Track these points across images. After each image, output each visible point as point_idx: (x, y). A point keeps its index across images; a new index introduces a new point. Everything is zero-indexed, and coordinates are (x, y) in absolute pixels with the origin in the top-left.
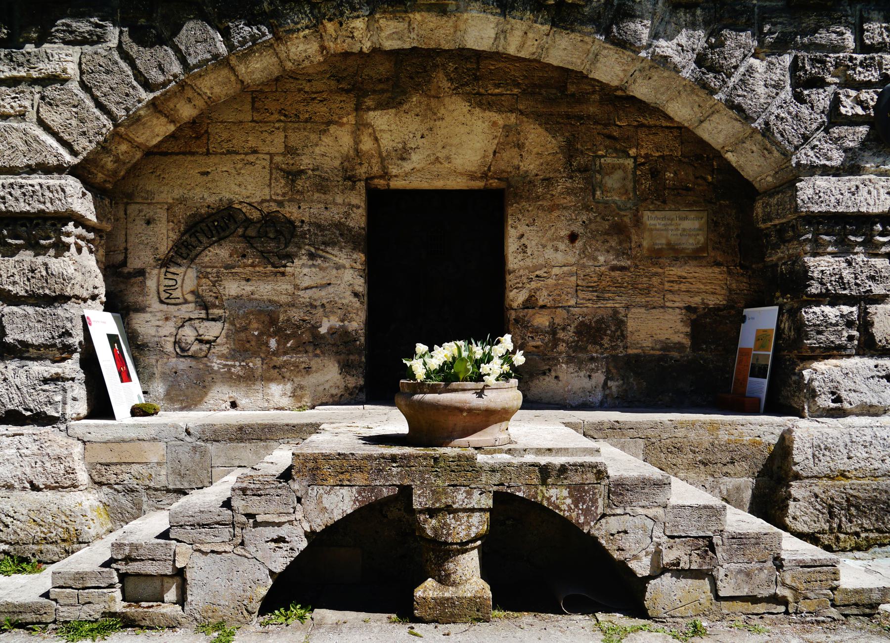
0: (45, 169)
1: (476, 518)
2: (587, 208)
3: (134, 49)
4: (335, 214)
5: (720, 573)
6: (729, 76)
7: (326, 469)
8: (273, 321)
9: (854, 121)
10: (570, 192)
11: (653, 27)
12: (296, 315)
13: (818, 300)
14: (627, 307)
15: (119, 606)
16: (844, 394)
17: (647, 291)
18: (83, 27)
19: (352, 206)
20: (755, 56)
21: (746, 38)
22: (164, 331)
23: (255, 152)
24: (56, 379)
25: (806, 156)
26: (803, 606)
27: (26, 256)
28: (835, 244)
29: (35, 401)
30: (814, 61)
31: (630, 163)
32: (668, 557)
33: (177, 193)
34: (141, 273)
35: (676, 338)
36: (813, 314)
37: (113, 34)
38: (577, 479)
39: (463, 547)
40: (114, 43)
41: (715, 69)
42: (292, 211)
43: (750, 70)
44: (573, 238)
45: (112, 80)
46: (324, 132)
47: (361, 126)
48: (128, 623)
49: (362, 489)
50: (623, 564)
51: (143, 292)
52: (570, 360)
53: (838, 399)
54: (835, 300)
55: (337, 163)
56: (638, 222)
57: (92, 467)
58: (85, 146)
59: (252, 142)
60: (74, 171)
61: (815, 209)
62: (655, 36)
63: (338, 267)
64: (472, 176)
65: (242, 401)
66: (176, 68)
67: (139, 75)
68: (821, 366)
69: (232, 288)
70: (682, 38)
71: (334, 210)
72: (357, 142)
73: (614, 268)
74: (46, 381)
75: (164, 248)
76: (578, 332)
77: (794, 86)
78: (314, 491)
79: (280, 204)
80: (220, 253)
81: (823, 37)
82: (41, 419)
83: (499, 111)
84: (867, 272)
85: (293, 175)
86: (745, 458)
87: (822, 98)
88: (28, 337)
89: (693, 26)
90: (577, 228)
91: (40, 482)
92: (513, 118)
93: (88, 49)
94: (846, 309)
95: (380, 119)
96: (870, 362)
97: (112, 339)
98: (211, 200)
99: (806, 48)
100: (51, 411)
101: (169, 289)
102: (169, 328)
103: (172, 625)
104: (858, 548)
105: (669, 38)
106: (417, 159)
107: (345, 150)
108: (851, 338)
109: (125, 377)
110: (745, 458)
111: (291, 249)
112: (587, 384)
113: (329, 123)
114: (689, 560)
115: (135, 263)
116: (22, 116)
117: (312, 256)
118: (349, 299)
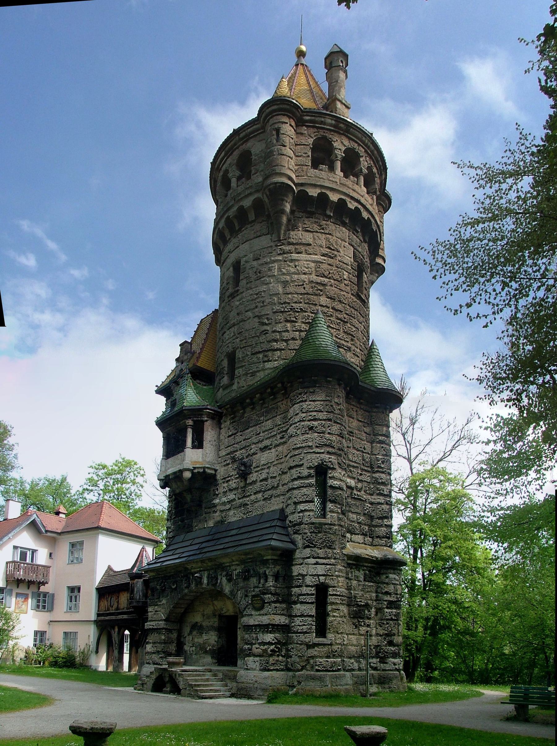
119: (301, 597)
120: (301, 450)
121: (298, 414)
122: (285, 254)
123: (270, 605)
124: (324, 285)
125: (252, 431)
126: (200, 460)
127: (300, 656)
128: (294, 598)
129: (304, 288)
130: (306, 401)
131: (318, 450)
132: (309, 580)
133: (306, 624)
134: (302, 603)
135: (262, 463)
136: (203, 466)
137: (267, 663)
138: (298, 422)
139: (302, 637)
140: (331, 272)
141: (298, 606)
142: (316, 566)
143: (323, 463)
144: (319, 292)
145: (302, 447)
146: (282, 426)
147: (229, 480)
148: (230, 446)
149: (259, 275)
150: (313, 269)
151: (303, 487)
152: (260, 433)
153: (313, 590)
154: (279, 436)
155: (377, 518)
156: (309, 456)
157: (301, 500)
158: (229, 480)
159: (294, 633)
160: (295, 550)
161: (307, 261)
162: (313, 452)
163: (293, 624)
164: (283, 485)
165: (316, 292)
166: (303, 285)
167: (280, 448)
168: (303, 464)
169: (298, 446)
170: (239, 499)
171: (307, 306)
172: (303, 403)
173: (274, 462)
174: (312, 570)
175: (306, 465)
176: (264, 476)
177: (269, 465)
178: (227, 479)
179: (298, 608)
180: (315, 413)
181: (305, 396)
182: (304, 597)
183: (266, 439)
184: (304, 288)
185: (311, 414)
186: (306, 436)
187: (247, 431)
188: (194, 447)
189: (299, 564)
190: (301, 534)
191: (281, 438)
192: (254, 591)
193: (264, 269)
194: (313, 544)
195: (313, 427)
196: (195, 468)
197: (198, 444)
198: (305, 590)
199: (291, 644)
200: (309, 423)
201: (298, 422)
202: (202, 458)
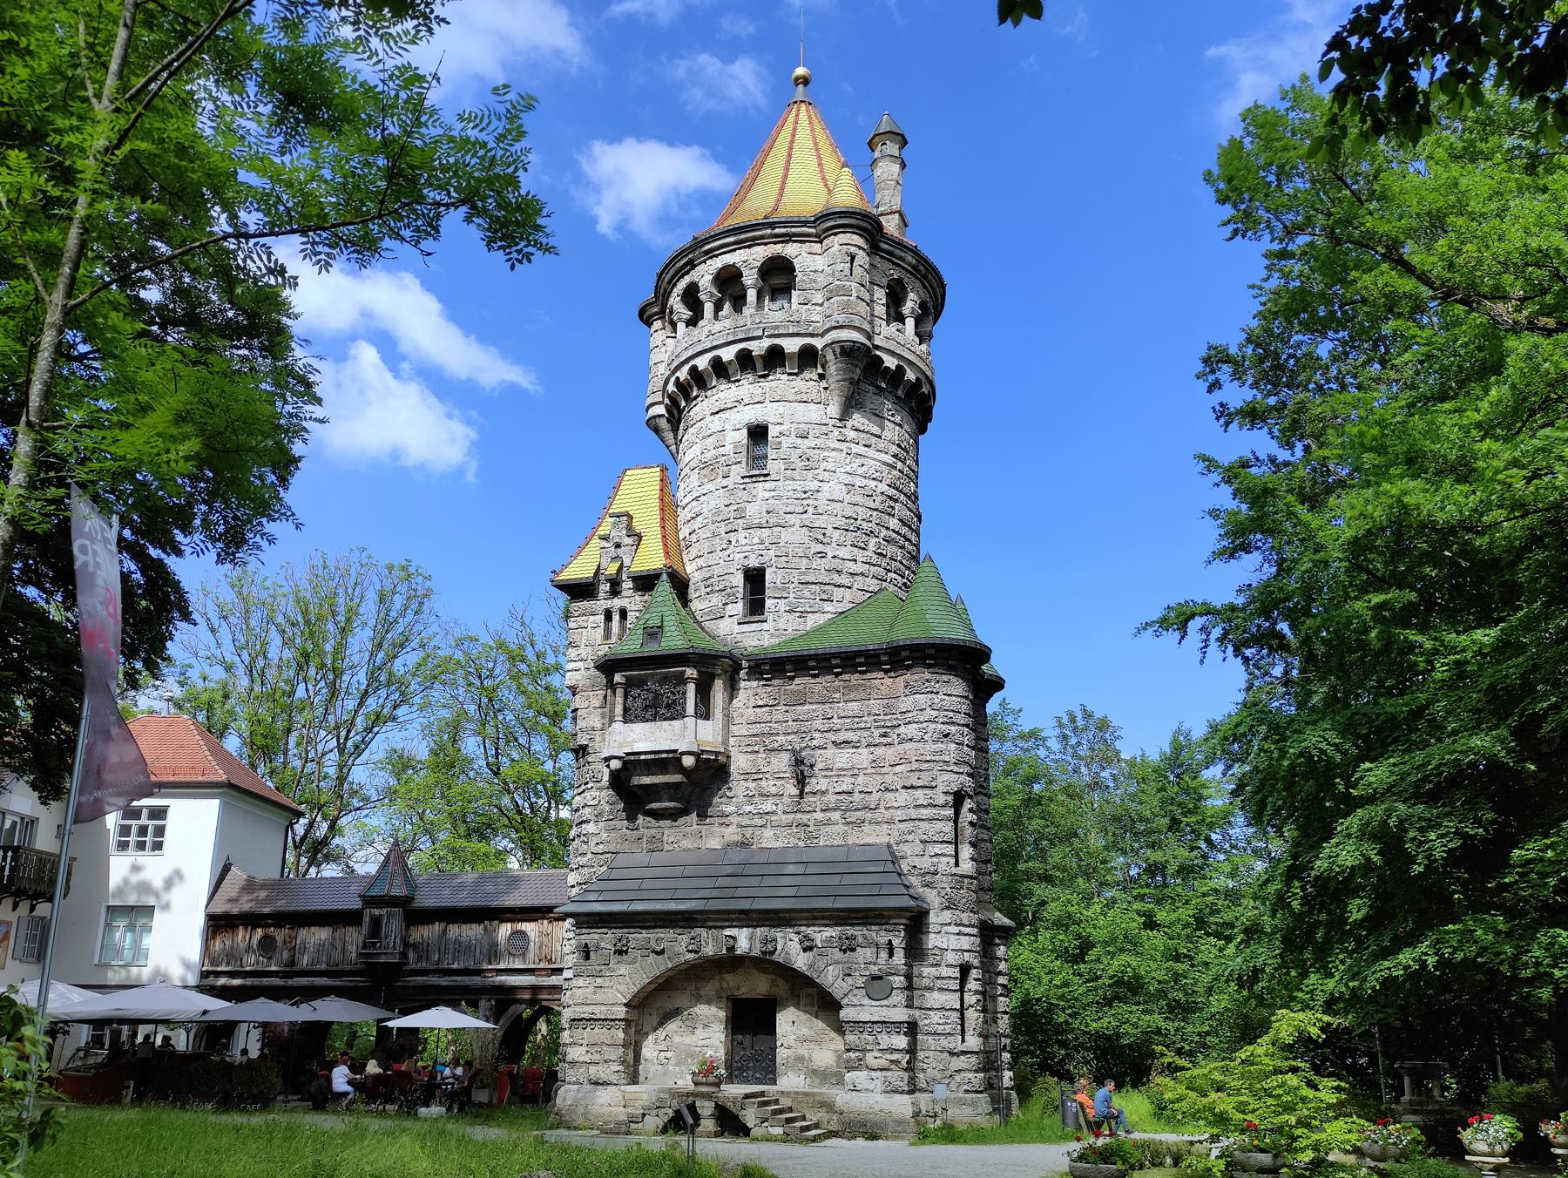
58: (629, 997)
87: (850, 980)
95: (728, 977)
106: (744, 990)
124: (896, 501)
125: (814, 711)
128: (926, 982)
131: (956, 769)
132: (951, 957)
134: (941, 989)
135: (841, 765)
139: (944, 1042)
141: (936, 994)
146: (882, 717)
153: (956, 973)
154: (876, 733)
156: (946, 776)
160: (927, 912)
163: (926, 1022)
164: (887, 808)
167: (880, 751)
170: (785, 812)
171: (877, 528)
174: (954, 942)
175: (941, 788)
176: (844, 788)
177: (856, 771)
179: (935, 999)
180: (951, 714)
186: (940, 745)
187: (799, 708)
188: (698, 715)
191: (881, 736)
197: (704, 712)
198: (945, 972)
200: (944, 727)
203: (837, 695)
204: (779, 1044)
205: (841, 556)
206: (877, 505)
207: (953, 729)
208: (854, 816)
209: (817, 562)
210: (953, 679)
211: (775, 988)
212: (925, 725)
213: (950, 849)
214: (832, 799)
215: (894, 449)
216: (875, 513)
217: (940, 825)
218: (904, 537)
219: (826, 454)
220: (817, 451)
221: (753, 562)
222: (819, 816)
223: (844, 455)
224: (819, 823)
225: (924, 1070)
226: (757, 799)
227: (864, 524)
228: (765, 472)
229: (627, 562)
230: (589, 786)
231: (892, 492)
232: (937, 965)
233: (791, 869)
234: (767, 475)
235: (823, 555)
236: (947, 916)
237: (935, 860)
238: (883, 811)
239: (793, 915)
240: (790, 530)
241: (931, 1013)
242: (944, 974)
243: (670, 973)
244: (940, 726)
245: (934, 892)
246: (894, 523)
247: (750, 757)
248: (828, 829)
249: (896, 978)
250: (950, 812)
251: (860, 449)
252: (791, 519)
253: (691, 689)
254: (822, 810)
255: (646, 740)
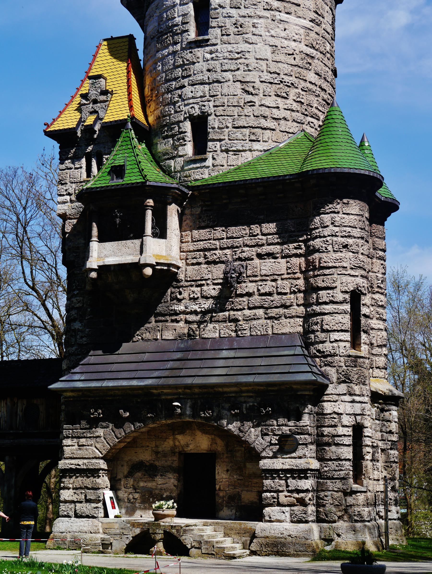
0: (96, 458)
1: (160, 535)
2: (231, 462)
3: (115, 429)
4: (169, 463)
5: (202, 548)
6: (245, 433)
7: (136, 525)
8: (151, 493)
9: (275, 444)
10: (227, 457)
11: (227, 422)
12: (157, 492)
13: (267, 491)
14: (242, 491)
15: (101, 549)
16: (271, 516)
17: (247, 486)
18: (104, 424)
19: (174, 461)
20: (253, 428)
21: (250, 424)
22: (125, 496)
23: (148, 446)
24: (97, 508)
25: (264, 454)
26: (218, 556)
27: (92, 478)
28: (271, 477)
29: (92, 513)
30: (266, 429)
31: (243, 449)
32: (193, 544)
33: (129, 458)
34: (120, 480)
35: (255, 500)
36: (265, 495)
37: (111, 425)
38: (177, 528)
39: (158, 541)
40: (111, 428)
41: (242, 432)
42: (157, 463)
43: (251, 432)
44: (228, 471)
45: (110, 437)
46: (165, 441)
47: (174, 439)
48: (102, 552)
49: (142, 528)
50: (185, 545)
51: (120, 485)
52: (226, 506)
53: (270, 518)
54: (270, 492)
55: (169, 449)
56: (245, 466)
57: (103, 529)
58: (104, 452)
59: (147, 444)
60: (102, 458)
61: (264, 468)
62: (228, 424)
63: (169, 478)
64: (207, 450)
65: (143, 516)
66: (123, 434)
67: (116, 436)
68: (267, 509)
69: (142, 484)
70: (234, 424)
71: (168, 462)
72: (174, 443)
73: (238, 480)
74: (94, 508)
75: (126, 473)
76: (228, 498)
77: (262, 435)
78: (134, 529)
79: (154, 461)
80: (139, 474)
81: (268, 422)
82: (93, 517)
83: (209, 434)
84: (278, 484)
85: (157, 453)
86: (248, 532)
87: (268, 438)
88: (91, 498)
89: (237, 421)
90: (229, 468)
91: (92, 531)
92: (213, 436)
93: (105, 429)
94: (272, 494)
95: (179, 437)
96: (279, 508)
97: (111, 498)
98: (137, 460)
99: (265, 425)
100: (95, 515)
101: (127, 484)
102: (126, 495)
103: (110, 553)
104: (266, 555)
105: (231, 424)
106: (191, 447)
107: (171, 445)
108: (274, 502)
109: (114, 507)
110: (248, 532)
111: (156, 474)
112: (230, 513)
113: (166, 438)
114: (197, 545)
115: (119, 477)
116: (91, 445)
117: (161, 475)
118: (173, 487)
119: (336, 438)
120: (334, 270)
121: (327, 226)
122: (272, 10)
123: (307, 447)
124: (313, 57)
126: (164, 253)
127: (338, 505)
129: (295, 58)
130: (338, 213)
131: (352, 273)
133: (343, 469)
135: (263, 272)
136: (169, 262)
137: (305, 514)
138: (329, 236)
140: (318, 42)
141: (333, 448)
142: (351, 404)
143: (357, 288)
144: (308, 65)
145: (335, 267)
147: (203, 285)
148: (202, 240)
149: (240, 29)
150: (303, 37)
151: (337, 313)
152: (258, 234)
153: (349, 431)
155: (378, 346)
156: (345, 279)
157: (335, 328)
158: (203, 285)
159: (329, 478)
160: (327, 386)
161: (297, 25)
162: (349, 274)
165: (306, 65)
166: (293, 54)
168: (336, 287)
169: (330, 265)
171: (296, 80)
172: (336, 215)
173: (283, 274)
176: (267, 290)
177: (276, 277)
178: (200, 282)
181: (338, 206)
182: (341, 438)
183: (269, 244)
184: (295, 58)
185: (345, 229)
186: (339, 254)
188: (155, 235)
189: (334, 401)
190: (335, 366)
191: (296, 248)
192: (278, 430)
193: (247, 22)
194: (349, 379)
195: (347, 245)
196: (158, 264)
199: (324, 491)
200: (343, 240)
201: (329, 236)
202: (166, 251)
203: (262, 217)
204: (217, 487)
205: (267, 104)
206: (298, 61)
207: (350, 241)
208: (273, 312)
209: (248, 110)
210: (351, 201)
211: (214, 445)
212: (328, 238)
213: (347, 336)
214: (256, 299)
215: (313, 16)
216: (296, 68)
217: (339, 317)
218: (320, 87)
219: (255, 21)
220: (247, 19)
221: (196, 112)
222: (247, 312)
223: (269, 21)
224: (247, 320)
225: (324, 506)
226: (200, 300)
227: (286, 79)
228: (206, 37)
229: (101, 114)
230: (76, 292)
231: (310, 51)
232: (335, 426)
233: (225, 354)
234: (208, 40)
235: (252, 104)
236: (343, 388)
237: (335, 344)
238: (296, 307)
239: (226, 389)
240: (226, 84)
241: (330, 462)
242: (340, 433)
243: (135, 434)
244: (340, 239)
245: (334, 370)
246: (311, 76)
247: (196, 267)
248: (255, 322)
249: (302, 436)
250: (347, 307)
251: (284, 16)
252: (228, 75)
253: (149, 214)
254: (250, 308)
255: (115, 255)
